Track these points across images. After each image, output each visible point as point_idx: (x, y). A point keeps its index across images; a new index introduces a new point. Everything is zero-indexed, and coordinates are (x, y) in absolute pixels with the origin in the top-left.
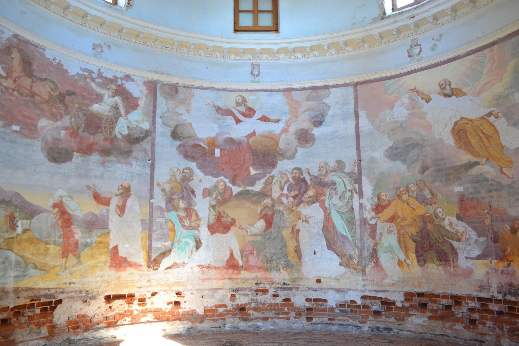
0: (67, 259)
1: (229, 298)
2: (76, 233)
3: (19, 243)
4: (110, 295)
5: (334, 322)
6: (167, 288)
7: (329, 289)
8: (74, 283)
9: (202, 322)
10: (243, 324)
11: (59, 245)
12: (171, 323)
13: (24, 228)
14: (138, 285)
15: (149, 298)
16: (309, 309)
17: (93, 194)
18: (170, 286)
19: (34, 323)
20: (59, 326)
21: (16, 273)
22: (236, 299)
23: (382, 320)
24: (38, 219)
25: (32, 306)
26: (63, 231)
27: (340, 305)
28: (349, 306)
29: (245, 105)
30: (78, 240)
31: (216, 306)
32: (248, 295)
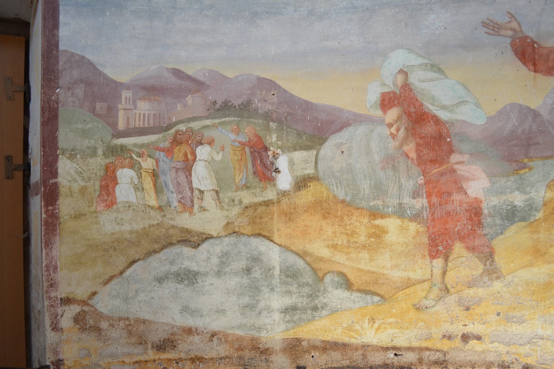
0: (446, 259)
2: (467, 179)
3: (289, 216)
8: (479, 338)
11: (415, 218)
13: (299, 173)
17: (513, 44)
21: (288, 301)
24: (339, 146)
26: (424, 173)
30: (478, 201)
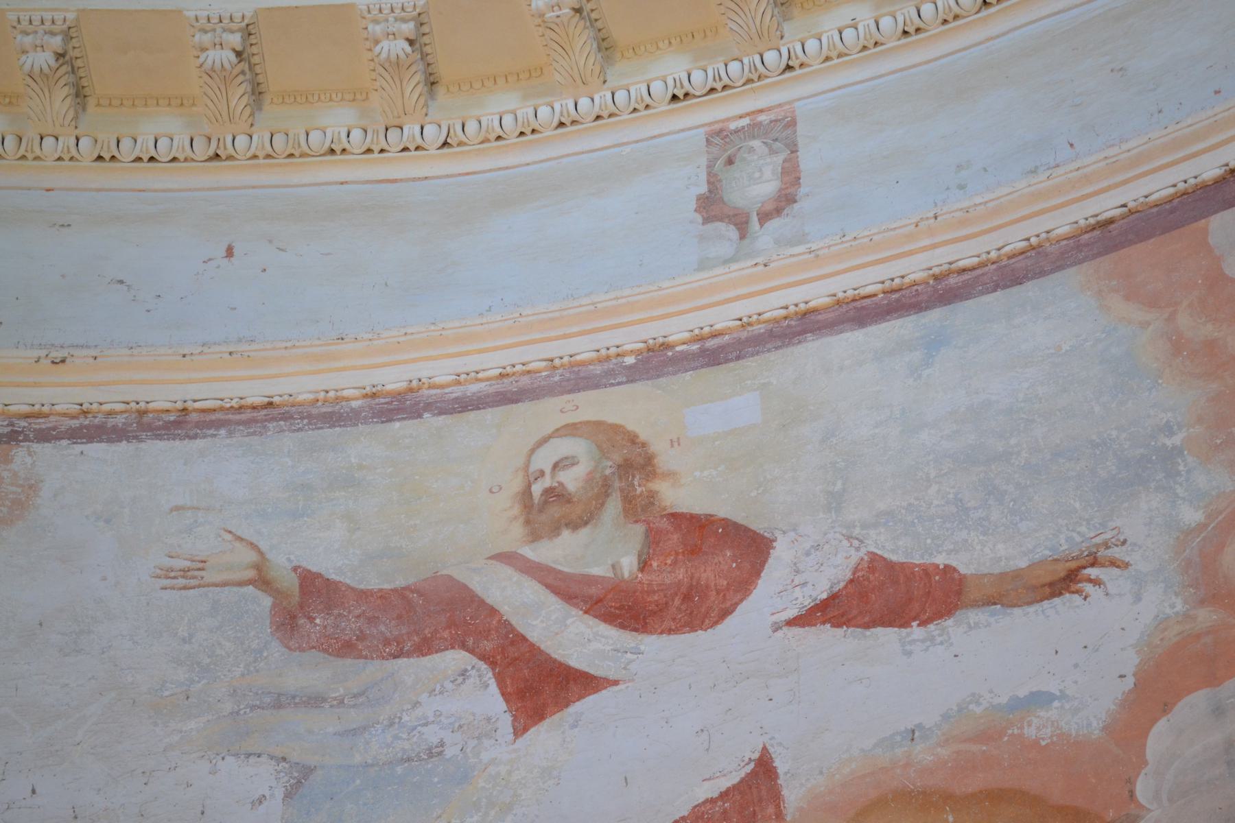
29: (638, 508)
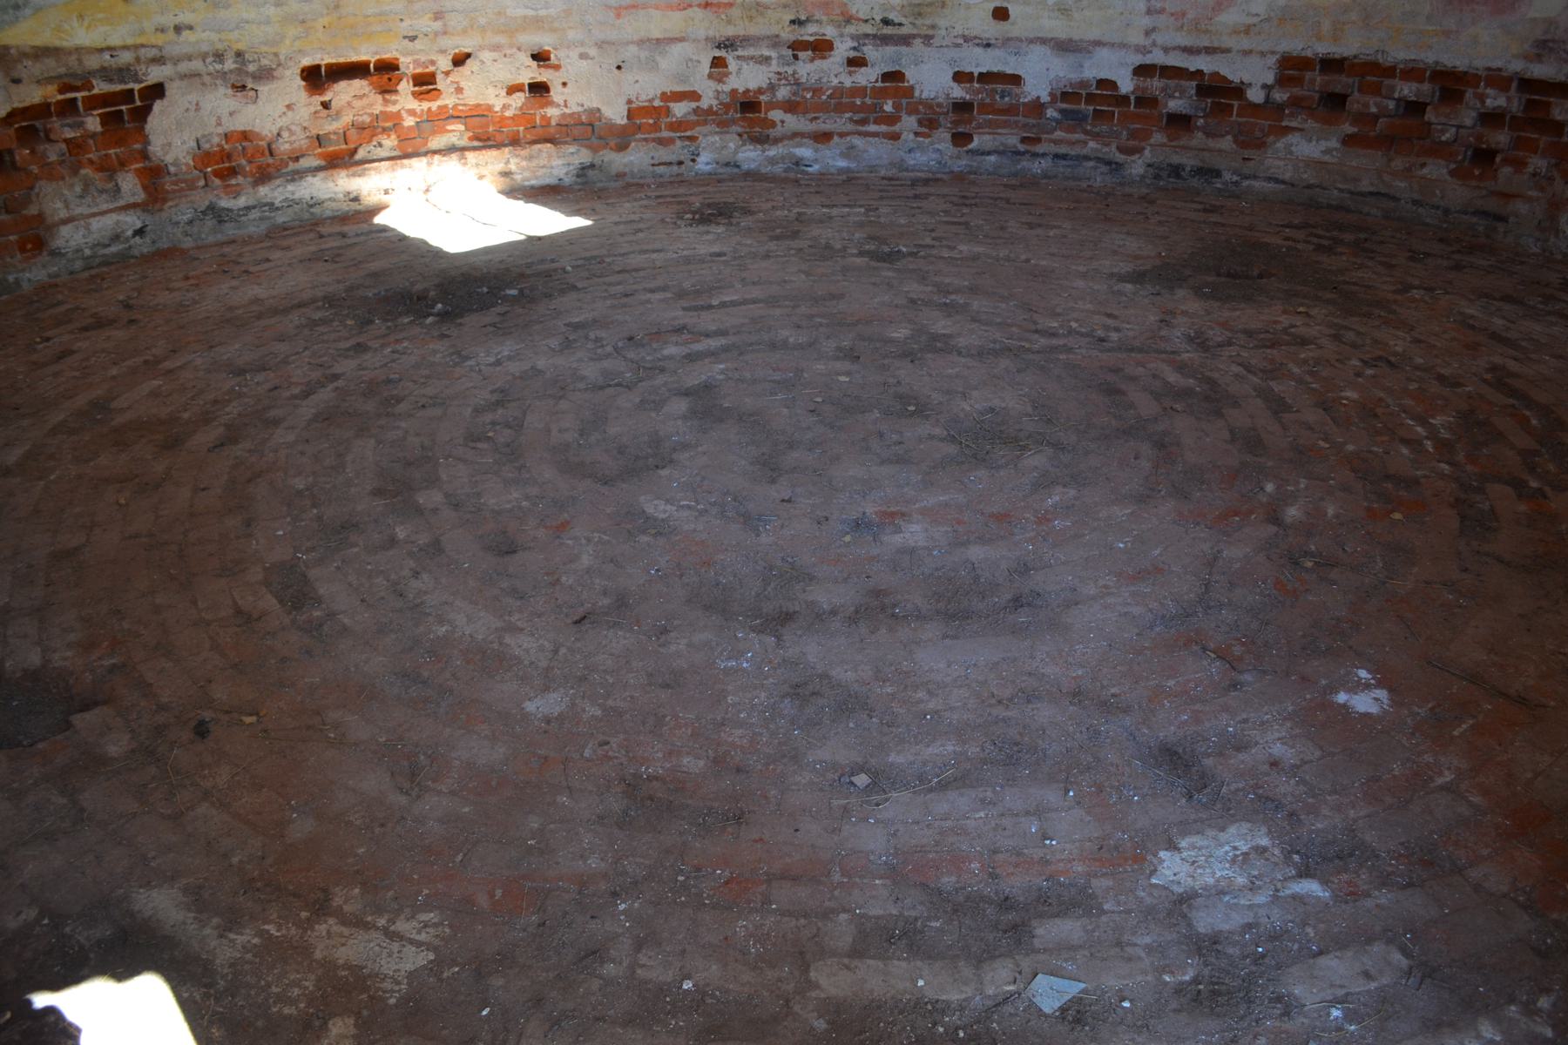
1: (707, 71)
4: (318, 67)
5: (1040, 149)
6: (501, 39)
7: (1031, 41)
8: (191, 28)
9: (622, 147)
10: (752, 155)
12: (524, 153)
14: (405, 27)
15: (447, 73)
16: (962, 107)
18: (511, 29)
19: (91, 162)
20: (172, 169)
22: (727, 75)
23: (1194, 143)
25: (68, 108)
27: (1064, 94)
28: (1091, 98)
31: (665, 97)
32: (767, 59)
